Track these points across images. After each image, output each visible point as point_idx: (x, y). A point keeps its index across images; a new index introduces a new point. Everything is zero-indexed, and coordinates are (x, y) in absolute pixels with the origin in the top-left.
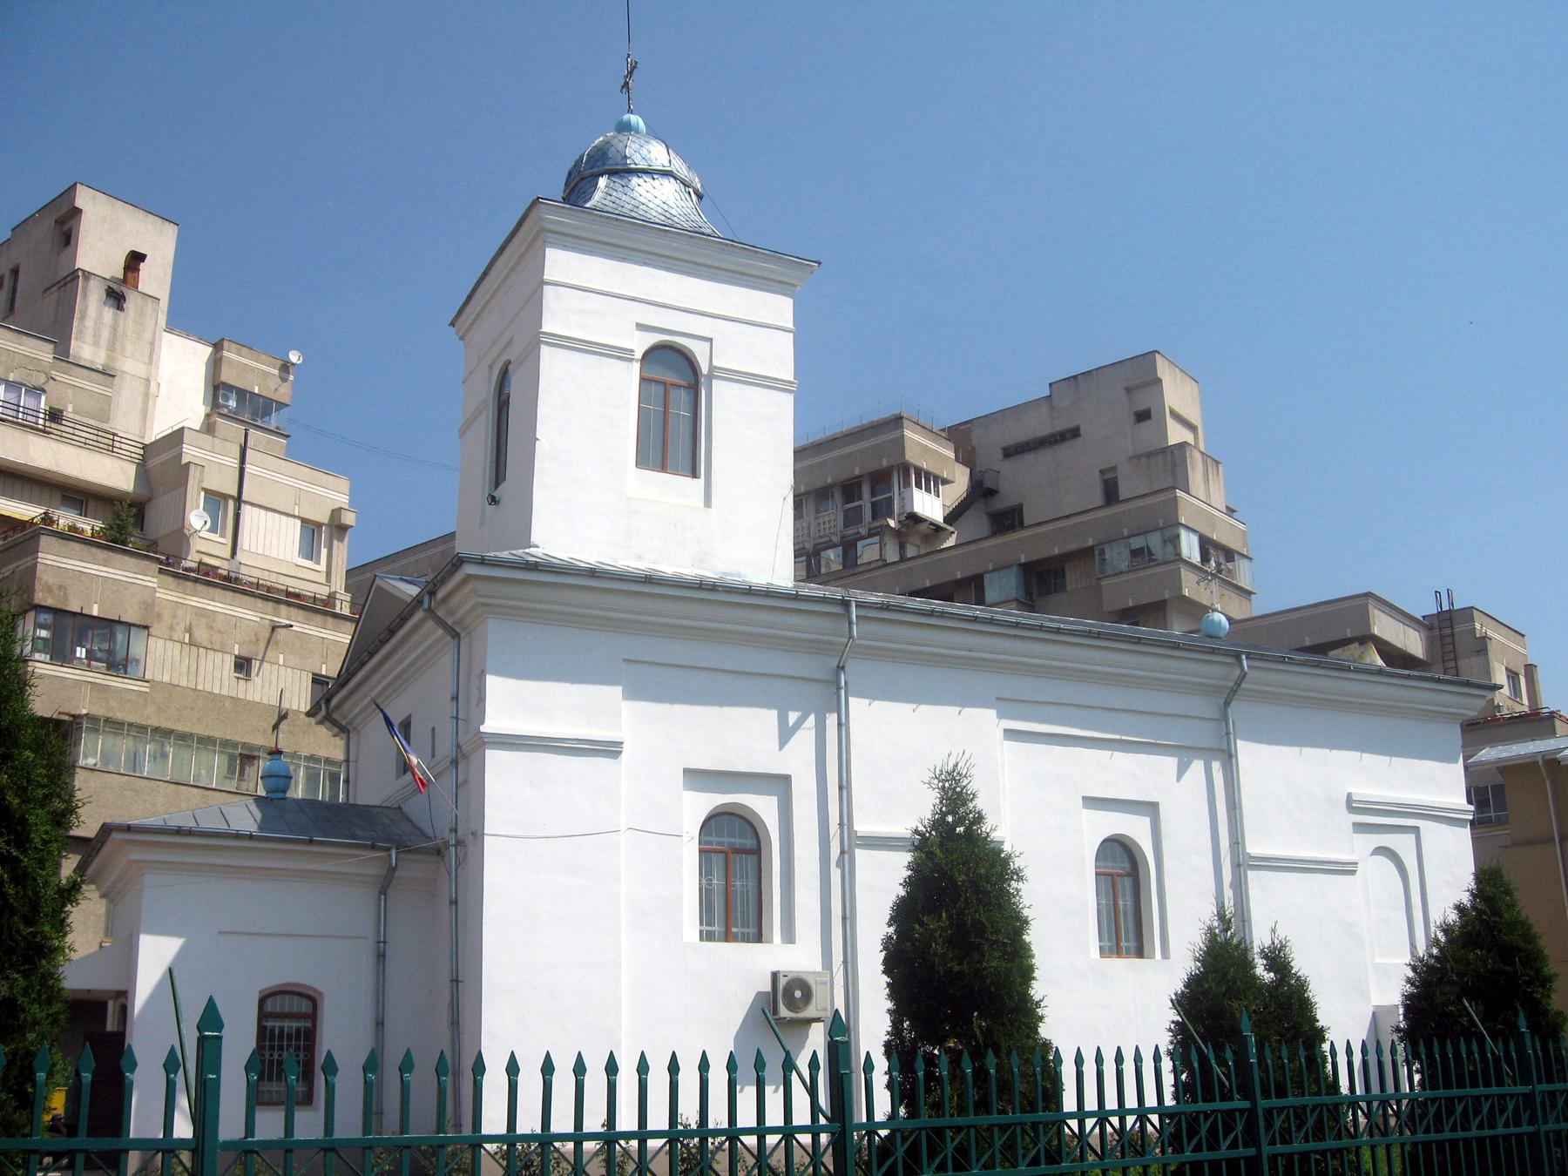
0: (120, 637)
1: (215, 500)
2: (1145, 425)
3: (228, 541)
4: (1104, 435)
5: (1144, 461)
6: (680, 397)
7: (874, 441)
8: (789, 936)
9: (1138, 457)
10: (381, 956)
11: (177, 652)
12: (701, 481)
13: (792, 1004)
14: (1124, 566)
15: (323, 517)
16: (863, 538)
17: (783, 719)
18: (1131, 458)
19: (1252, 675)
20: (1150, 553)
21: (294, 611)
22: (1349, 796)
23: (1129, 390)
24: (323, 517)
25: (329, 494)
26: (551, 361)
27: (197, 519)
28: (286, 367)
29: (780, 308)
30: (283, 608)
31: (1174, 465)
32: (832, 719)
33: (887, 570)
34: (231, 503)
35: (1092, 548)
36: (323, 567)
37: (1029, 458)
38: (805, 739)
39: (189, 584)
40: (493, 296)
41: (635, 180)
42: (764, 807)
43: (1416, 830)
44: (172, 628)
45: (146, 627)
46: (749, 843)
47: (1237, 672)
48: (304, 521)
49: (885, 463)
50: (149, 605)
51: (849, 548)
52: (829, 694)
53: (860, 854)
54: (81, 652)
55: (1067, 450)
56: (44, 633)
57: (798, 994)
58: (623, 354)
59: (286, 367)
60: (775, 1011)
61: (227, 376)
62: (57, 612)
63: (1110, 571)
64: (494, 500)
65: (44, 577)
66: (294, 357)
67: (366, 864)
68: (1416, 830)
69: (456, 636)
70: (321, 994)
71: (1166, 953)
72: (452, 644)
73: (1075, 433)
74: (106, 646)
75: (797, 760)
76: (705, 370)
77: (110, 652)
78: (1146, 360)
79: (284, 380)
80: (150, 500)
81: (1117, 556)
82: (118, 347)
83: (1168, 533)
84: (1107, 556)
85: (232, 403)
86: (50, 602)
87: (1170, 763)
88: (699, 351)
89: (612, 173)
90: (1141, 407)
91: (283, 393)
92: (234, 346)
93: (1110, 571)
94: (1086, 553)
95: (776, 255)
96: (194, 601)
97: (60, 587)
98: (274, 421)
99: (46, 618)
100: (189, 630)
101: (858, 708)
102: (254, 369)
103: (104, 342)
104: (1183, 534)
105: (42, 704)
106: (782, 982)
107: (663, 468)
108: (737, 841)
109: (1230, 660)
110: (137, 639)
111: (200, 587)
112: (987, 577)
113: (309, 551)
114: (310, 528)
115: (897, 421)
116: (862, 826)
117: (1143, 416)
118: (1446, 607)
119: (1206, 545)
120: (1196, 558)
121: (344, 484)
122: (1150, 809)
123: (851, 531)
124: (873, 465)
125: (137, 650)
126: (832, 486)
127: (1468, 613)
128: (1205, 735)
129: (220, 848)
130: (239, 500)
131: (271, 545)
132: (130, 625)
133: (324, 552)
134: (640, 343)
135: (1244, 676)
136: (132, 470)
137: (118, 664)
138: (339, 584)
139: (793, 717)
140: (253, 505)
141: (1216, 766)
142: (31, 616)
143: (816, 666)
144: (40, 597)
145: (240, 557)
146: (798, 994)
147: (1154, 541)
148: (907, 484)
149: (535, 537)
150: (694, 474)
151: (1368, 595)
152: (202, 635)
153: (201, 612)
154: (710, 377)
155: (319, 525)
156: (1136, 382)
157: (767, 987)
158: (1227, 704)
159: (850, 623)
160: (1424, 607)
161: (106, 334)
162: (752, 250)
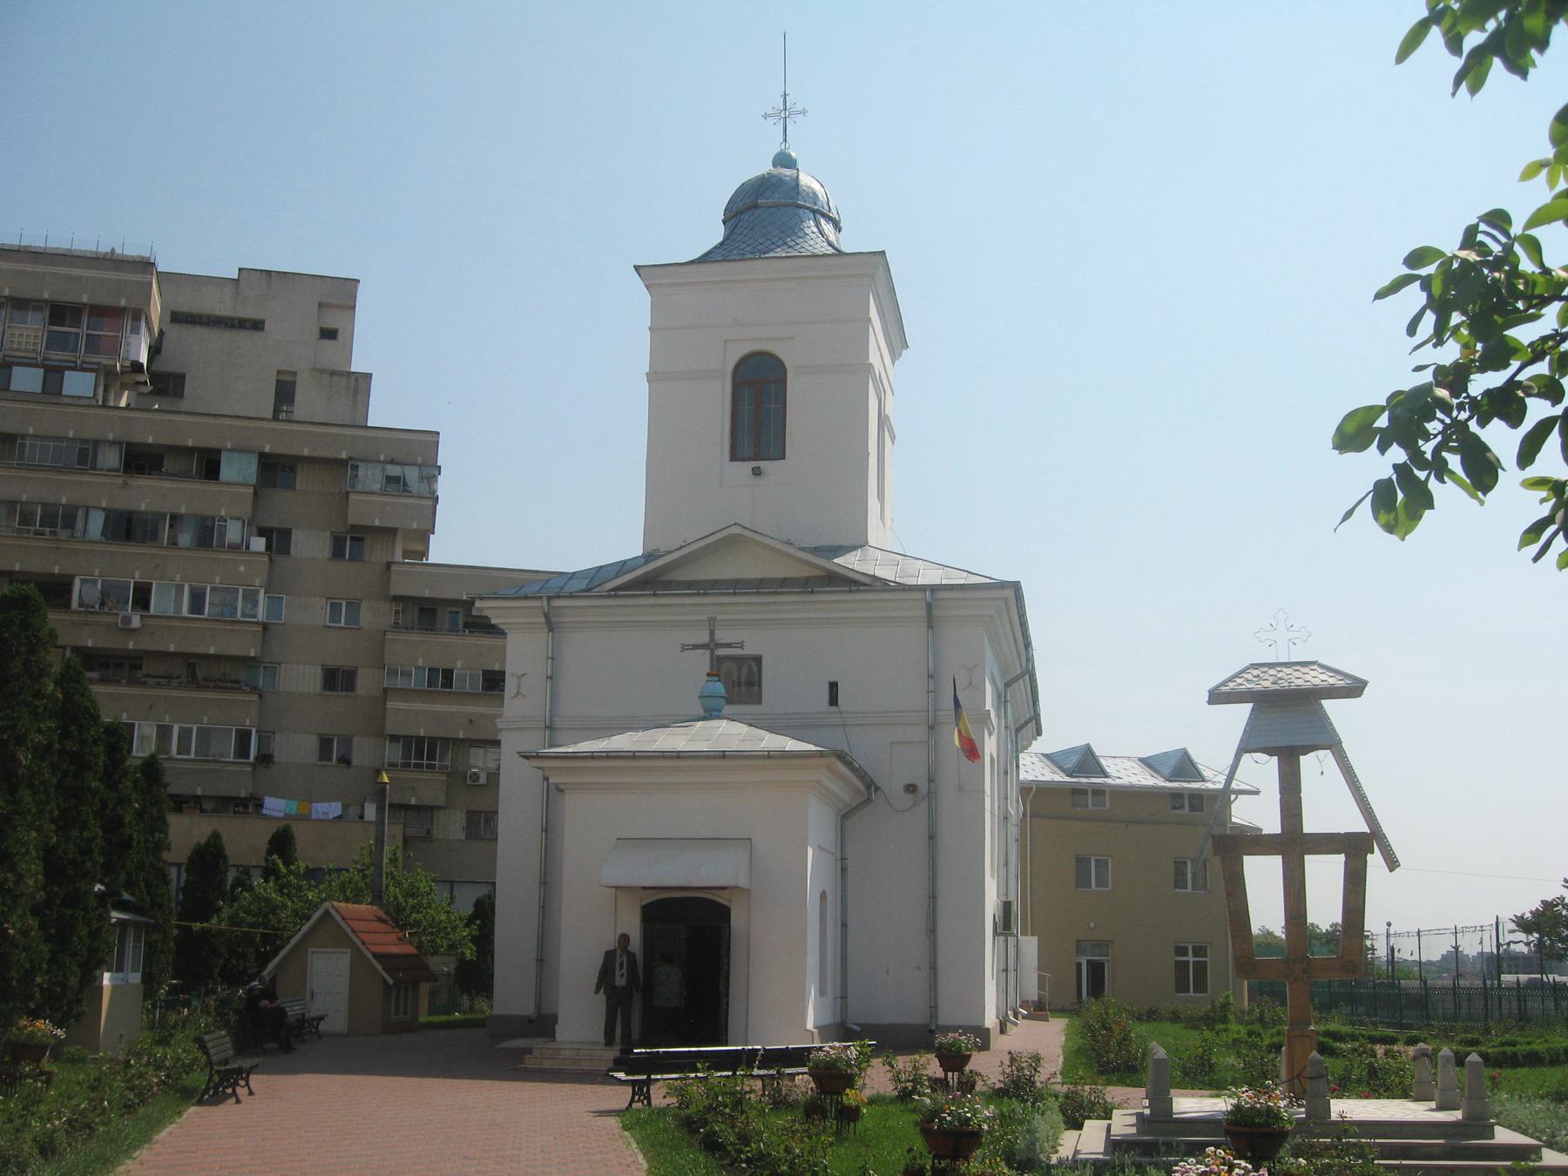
2: (328, 343)
4: (288, 340)
5: (326, 376)
7: (110, 275)
9: (322, 371)
10: (844, 870)
14: (376, 487)
16: (74, 369)
18: (314, 370)
20: (405, 484)
23: (320, 305)
31: (356, 392)
33: (92, 411)
35: (341, 464)
40: (742, 281)
49: (123, 303)
51: (54, 374)
55: (244, 339)
69: (930, 626)
73: (258, 325)
81: (371, 477)
84: (361, 472)
90: (329, 324)
93: (359, 487)
112: (224, 457)
115: (147, 265)
117: (329, 334)
123: (58, 356)
124: (103, 299)
126: (46, 301)
147: (412, 474)
148: (136, 330)
156: (333, 302)
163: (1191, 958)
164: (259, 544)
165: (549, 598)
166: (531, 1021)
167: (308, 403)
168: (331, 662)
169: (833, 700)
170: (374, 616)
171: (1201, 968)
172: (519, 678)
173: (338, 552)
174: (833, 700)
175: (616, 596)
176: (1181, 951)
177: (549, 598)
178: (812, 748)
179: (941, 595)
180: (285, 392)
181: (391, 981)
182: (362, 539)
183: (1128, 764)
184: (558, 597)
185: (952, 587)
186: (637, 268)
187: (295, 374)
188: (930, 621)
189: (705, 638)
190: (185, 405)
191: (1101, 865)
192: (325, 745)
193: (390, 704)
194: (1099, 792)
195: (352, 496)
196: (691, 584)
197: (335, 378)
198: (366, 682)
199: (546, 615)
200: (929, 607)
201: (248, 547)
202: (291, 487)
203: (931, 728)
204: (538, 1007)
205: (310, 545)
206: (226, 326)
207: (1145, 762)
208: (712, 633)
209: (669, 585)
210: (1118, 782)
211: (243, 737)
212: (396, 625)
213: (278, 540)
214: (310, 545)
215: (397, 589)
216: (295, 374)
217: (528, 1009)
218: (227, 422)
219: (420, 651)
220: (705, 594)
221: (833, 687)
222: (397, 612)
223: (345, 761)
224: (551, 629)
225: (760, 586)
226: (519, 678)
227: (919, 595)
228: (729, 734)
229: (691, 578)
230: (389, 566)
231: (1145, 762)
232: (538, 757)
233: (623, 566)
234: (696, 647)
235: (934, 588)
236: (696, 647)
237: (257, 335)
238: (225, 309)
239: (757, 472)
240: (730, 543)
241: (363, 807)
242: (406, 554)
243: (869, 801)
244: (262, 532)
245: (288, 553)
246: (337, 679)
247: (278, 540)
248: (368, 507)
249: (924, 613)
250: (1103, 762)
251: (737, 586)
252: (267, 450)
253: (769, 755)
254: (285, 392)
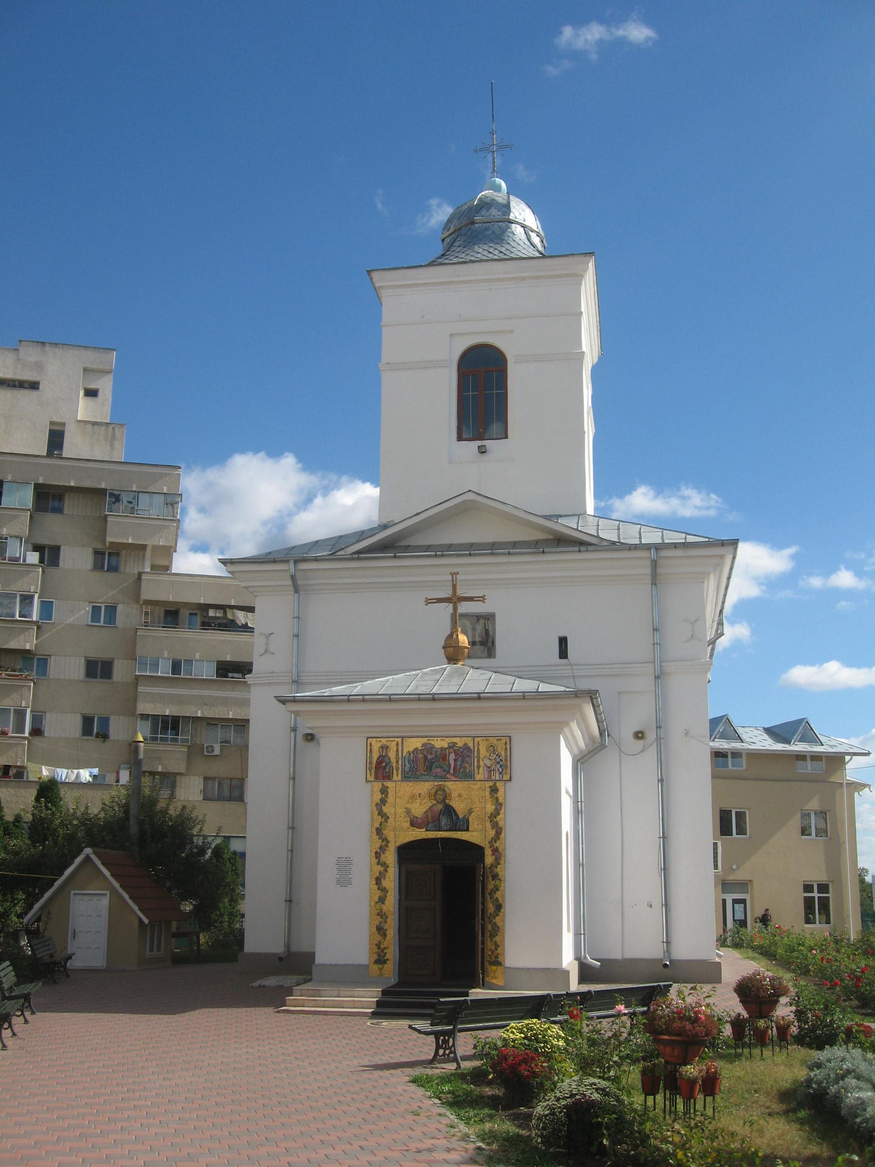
5: (89, 427)
69: (654, 583)
73: (34, 386)
90: (92, 386)
163: (816, 894)
164: (33, 558)
165: (296, 562)
166: (281, 959)
167: (75, 445)
168: (94, 654)
169: (563, 653)
170: (128, 615)
171: (824, 905)
172: (268, 636)
173: (98, 566)
174: (563, 653)
175: (359, 559)
176: (808, 888)
177: (296, 562)
178: (563, 689)
179: (664, 553)
180: (56, 439)
181: (146, 921)
182: (118, 554)
183: (756, 732)
184: (304, 560)
185: (675, 546)
187: (64, 424)
188: (654, 579)
189: (447, 593)
191: (740, 816)
192: (87, 722)
193: (141, 689)
194: (736, 754)
195: (109, 519)
196: (428, 548)
197: (95, 426)
198: (120, 672)
199: (293, 578)
200: (654, 564)
201: (24, 560)
202: (59, 510)
203: (657, 678)
204: (288, 946)
205: (76, 558)
206: (9, 386)
207: (769, 731)
208: (454, 587)
209: (407, 548)
210: (753, 747)
211: (20, 714)
212: (146, 624)
213: (50, 555)
214: (76, 558)
215: (146, 595)
216: (64, 424)
217: (276, 947)
218: (9, 458)
219: (163, 645)
220: (442, 556)
221: (563, 642)
222: (147, 613)
223: (104, 736)
224: (296, 591)
225: (493, 548)
226: (268, 636)
227: (645, 554)
228: (475, 679)
229: (427, 543)
230: (140, 575)
231: (769, 731)
232: (294, 700)
233: (361, 535)
234: (440, 600)
235: (658, 547)
236: (440, 600)
237: (33, 394)
239: (482, 451)
240: (465, 508)
241: (118, 773)
242: (153, 567)
243: (602, 746)
244: (37, 548)
245: (58, 566)
246: (99, 669)
247: (50, 555)
248: (120, 530)
250: (740, 731)
251: (471, 549)
252: (41, 481)
253: (524, 696)
254: (56, 439)
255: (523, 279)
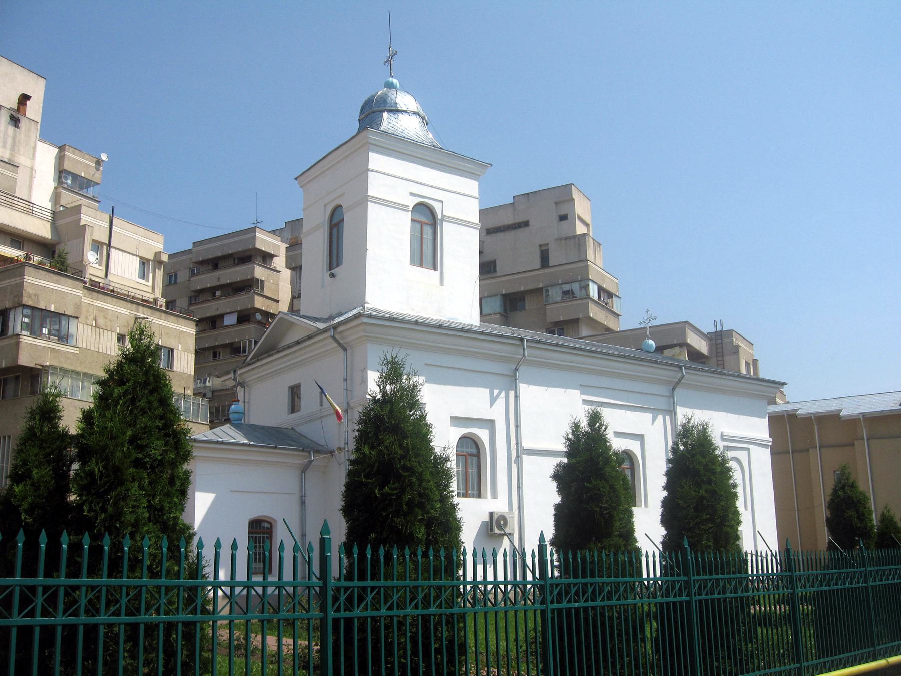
0: (63, 323)
1: (97, 246)
2: (564, 223)
3: (103, 268)
4: (543, 227)
5: (563, 242)
6: (428, 230)
8: (494, 496)
9: (560, 239)
10: (303, 503)
11: (89, 331)
12: (439, 272)
13: (499, 527)
14: (558, 299)
15: (150, 256)
17: (491, 393)
19: (687, 376)
20: (573, 293)
21: (145, 309)
22: (722, 433)
23: (556, 203)
24: (150, 256)
25: (154, 244)
26: (373, 210)
27: (91, 257)
28: (98, 162)
29: (471, 186)
30: (141, 308)
32: (512, 393)
34: (105, 247)
35: (541, 289)
36: (150, 284)
37: (500, 236)
38: (501, 401)
39: (95, 294)
41: (401, 115)
42: (483, 434)
43: (748, 449)
44: (86, 318)
45: (77, 318)
46: (474, 451)
47: (680, 375)
48: (141, 258)
50: (78, 306)
52: (511, 381)
53: (525, 458)
54: (45, 331)
55: (521, 233)
56: (26, 320)
57: (502, 522)
58: (403, 208)
59: (98, 162)
60: (492, 530)
61: (67, 166)
62: (33, 308)
63: (550, 301)
64: (333, 276)
65: (28, 290)
66: (104, 157)
67: (298, 459)
68: (748, 449)
69: (345, 349)
70: (275, 521)
71: (646, 506)
72: (342, 353)
73: (526, 224)
74: (57, 327)
75: (497, 413)
76: (440, 217)
77: (58, 331)
78: (567, 188)
79: (97, 169)
80: (59, 243)
81: (555, 294)
82: (16, 148)
83: (583, 284)
84: (550, 293)
85: (69, 182)
86: (30, 303)
87: (649, 416)
88: (437, 207)
89: (390, 111)
90: (562, 213)
91: (97, 177)
92: (71, 149)
93: (550, 301)
94: (538, 291)
95: (472, 161)
96: (98, 304)
97: (35, 295)
98: (91, 192)
99: (27, 312)
100: (95, 319)
101: (523, 388)
102: (81, 163)
103: (8, 146)
104: (591, 284)
105: (25, 359)
106: (495, 517)
107: (421, 265)
108: (469, 450)
109: (677, 369)
110: (73, 323)
111: (100, 296)
113: (143, 275)
114: (144, 263)
116: (526, 444)
117: (563, 218)
118: (719, 329)
119: (600, 289)
120: (596, 298)
121: (161, 238)
122: (640, 437)
125: (72, 330)
127: (730, 333)
128: (662, 403)
129: (234, 450)
130: (109, 246)
131: (125, 271)
132: (69, 316)
133: (151, 275)
134: (412, 202)
135: (683, 376)
136: (48, 225)
137: (64, 338)
138: (158, 293)
139: (496, 392)
140: (116, 248)
141: (668, 418)
142: (19, 310)
143: (505, 368)
144: (26, 301)
145: (109, 277)
146: (502, 522)
147: (575, 287)
149: (369, 297)
150: (435, 269)
151: (686, 323)
152: (101, 322)
153: (101, 310)
154: (442, 220)
155: (148, 260)
156: (560, 200)
157: (487, 519)
158: (674, 389)
159: (524, 349)
160: (709, 329)
161: (9, 141)
162: (462, 158)
177: (235, 372)
179: (340, 329)
186: (296, 179)
190: (498, 274)
202: (523, 308)
237: (527, 229)
238: (509, 221)
239: (333, 276)
249: (335, 344)
255: (347, 156)
